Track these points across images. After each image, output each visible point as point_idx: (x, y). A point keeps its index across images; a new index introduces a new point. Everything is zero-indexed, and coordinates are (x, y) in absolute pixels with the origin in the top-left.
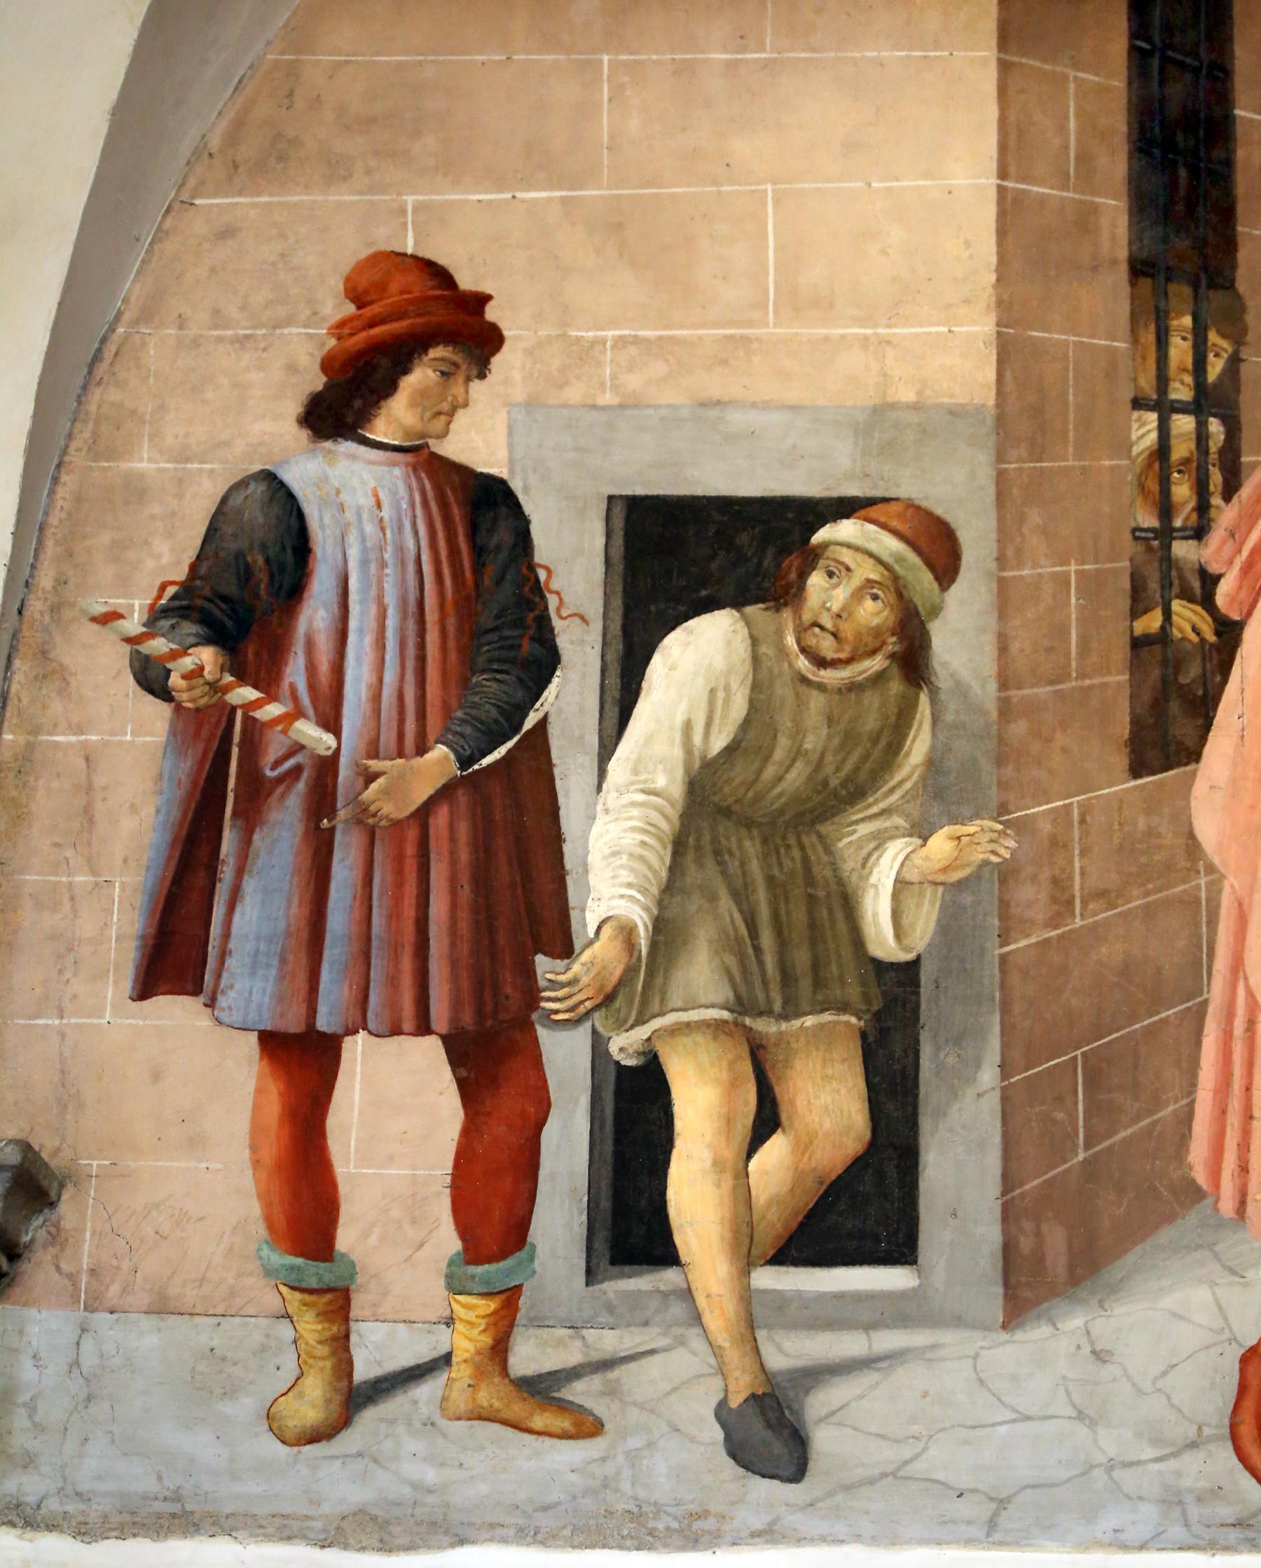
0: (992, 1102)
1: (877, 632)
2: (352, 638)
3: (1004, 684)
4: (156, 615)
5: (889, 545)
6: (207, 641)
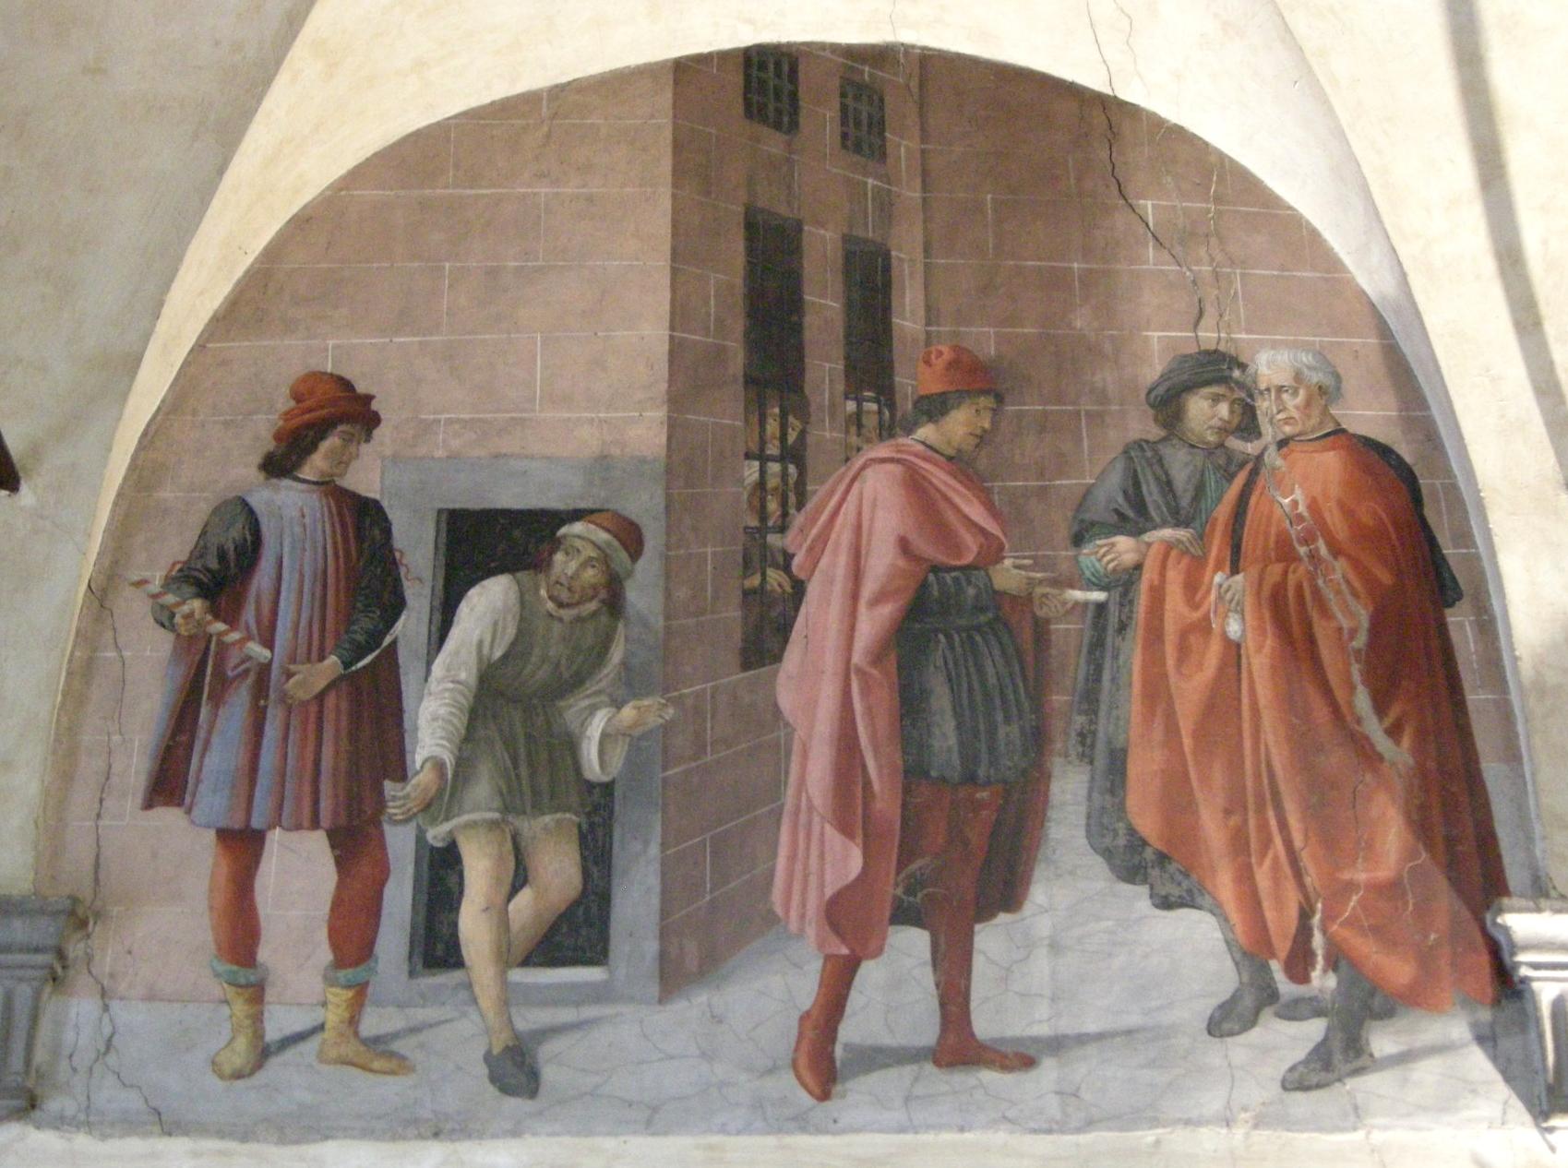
0: (656, 866)
1: (594, 587)
2: (283, 594)
3: (668, 617)
4: (170, 582)
5: (603, 536)
6: (197, 596)
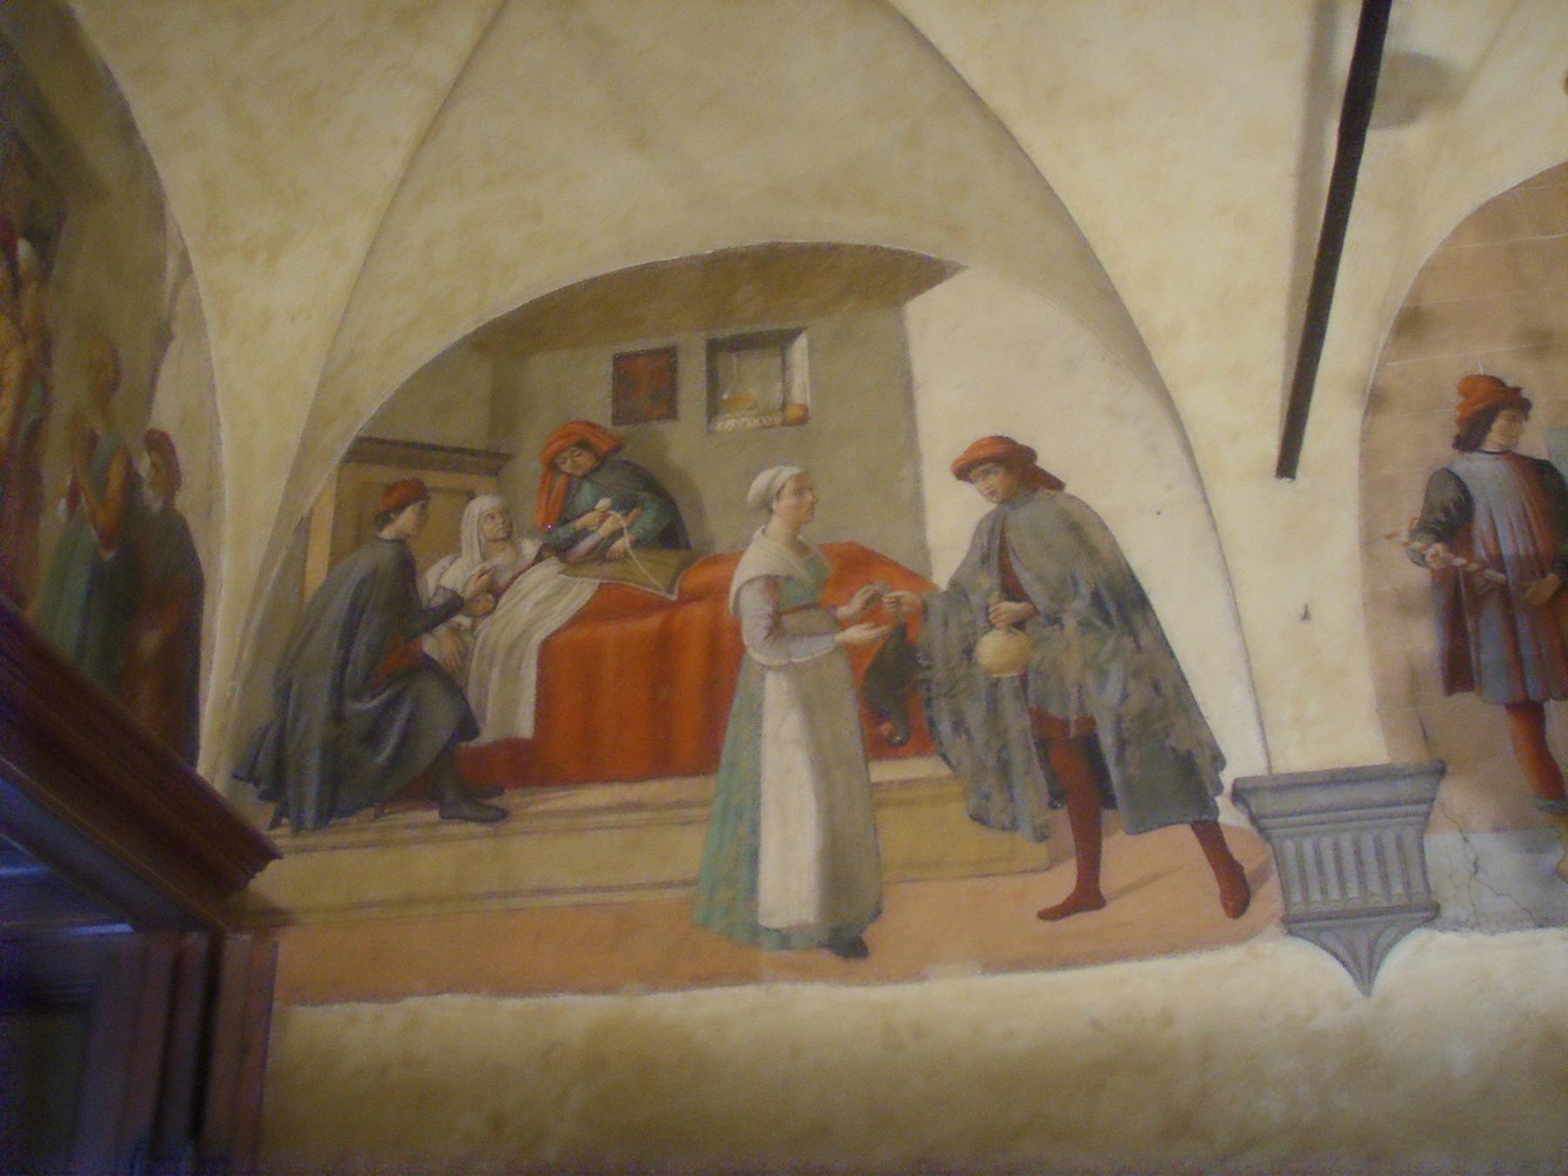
4: (1413, 534)
6: (1437, 541)
